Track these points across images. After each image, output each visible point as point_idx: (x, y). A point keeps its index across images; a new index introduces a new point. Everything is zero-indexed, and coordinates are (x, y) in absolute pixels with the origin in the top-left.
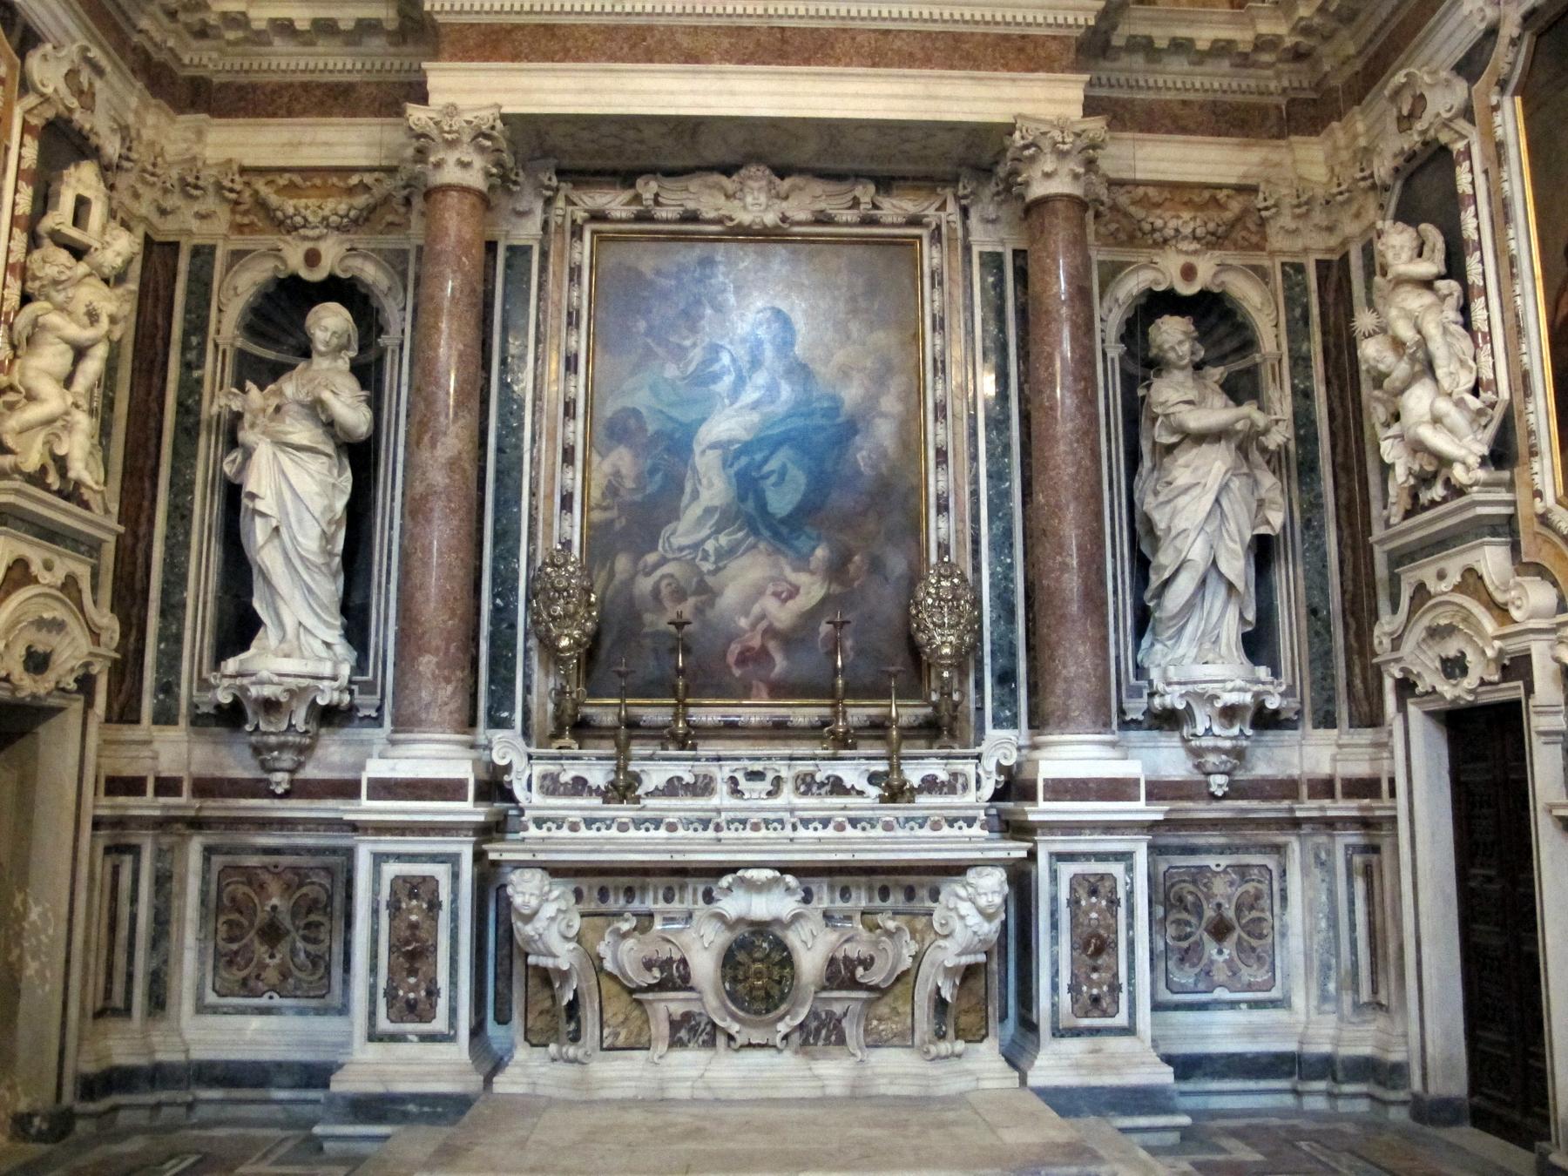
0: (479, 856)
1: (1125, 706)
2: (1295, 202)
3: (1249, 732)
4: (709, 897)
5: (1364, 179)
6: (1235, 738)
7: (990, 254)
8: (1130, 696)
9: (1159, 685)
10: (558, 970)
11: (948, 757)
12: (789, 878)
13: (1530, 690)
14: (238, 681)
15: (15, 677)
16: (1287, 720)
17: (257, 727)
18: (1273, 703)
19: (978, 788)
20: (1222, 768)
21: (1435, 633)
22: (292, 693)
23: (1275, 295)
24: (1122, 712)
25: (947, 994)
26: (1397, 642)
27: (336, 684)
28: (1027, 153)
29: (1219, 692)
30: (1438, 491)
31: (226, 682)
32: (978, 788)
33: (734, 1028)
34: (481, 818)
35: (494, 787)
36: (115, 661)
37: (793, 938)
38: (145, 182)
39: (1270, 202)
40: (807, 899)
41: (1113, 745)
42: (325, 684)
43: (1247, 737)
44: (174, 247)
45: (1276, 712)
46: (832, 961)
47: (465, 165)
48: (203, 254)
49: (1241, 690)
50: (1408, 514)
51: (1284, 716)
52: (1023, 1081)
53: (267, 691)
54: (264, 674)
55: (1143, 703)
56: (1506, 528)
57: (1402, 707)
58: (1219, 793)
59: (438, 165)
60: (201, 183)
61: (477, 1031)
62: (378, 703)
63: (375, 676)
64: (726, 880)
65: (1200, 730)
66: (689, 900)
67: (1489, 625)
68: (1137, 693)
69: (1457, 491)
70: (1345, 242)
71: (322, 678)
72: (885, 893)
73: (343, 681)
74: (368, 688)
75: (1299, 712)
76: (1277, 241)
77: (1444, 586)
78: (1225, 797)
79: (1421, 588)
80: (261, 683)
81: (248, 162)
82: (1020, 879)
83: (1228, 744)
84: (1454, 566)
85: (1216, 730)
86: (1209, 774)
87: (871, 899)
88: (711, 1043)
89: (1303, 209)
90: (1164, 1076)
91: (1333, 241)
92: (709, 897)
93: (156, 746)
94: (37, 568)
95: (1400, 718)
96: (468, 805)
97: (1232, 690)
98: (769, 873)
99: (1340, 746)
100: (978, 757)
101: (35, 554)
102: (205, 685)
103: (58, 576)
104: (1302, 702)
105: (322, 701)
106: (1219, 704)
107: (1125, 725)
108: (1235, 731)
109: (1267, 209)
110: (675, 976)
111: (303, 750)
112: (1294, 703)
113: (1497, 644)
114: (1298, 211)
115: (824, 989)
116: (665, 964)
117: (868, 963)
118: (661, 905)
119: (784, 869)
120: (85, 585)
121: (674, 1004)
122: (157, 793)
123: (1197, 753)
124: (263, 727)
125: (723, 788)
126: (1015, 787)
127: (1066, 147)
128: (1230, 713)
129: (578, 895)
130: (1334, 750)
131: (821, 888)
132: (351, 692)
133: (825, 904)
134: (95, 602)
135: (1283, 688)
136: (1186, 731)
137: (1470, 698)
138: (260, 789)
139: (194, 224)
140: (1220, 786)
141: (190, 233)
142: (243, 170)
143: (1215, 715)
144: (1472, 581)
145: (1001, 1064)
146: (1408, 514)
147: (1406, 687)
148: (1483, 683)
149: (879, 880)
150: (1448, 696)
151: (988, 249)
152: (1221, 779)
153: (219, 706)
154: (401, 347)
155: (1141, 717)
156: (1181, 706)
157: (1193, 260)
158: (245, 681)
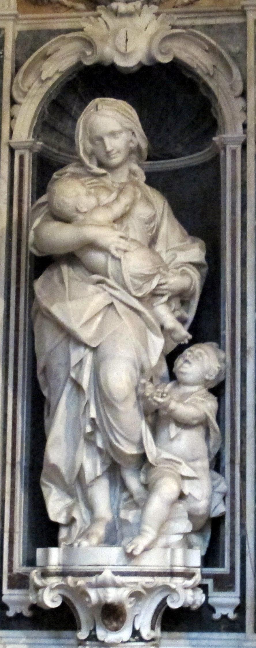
17: (93, 637)
22: (136, 595)
27: (190, 583)
31: (54, 581)
42: (177, 582)
54: (107, 574)
62: (237, 601)
63: (232, 568)
80: (103, 585)
105: (174, 604)
124: (101, 634)
132: (204, 588)
158: (81, 582)
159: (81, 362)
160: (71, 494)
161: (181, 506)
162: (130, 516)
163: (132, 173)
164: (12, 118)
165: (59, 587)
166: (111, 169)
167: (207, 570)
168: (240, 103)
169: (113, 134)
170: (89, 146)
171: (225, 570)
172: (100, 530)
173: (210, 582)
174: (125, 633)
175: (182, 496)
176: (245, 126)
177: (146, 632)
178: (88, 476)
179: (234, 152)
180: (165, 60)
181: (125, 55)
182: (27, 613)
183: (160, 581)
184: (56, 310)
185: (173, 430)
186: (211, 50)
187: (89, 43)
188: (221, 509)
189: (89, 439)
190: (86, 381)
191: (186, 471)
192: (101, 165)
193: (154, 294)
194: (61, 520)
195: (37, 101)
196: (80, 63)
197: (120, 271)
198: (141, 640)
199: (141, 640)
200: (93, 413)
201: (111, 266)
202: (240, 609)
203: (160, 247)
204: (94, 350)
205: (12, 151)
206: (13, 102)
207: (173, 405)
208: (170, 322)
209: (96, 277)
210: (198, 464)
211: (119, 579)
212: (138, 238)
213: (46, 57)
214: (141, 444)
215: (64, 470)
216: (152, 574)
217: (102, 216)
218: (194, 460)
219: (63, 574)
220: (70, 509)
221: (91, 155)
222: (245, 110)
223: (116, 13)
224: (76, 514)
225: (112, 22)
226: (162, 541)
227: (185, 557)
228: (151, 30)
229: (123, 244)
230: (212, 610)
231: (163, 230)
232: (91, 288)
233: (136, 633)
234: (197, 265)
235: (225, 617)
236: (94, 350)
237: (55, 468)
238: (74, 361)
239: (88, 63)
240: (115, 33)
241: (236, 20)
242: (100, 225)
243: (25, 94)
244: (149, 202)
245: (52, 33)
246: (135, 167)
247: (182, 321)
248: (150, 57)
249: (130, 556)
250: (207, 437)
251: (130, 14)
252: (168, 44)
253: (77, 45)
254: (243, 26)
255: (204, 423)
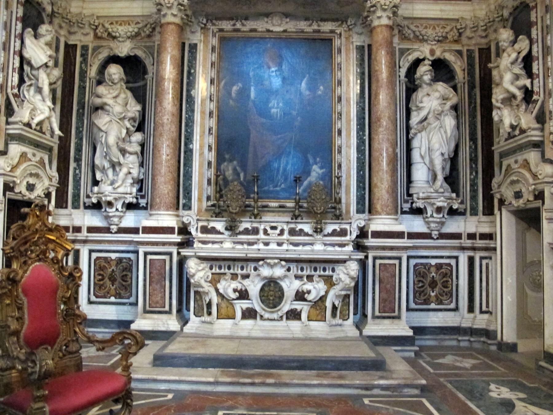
0: (179, 253)
1: (403, 206)
2: (472, 26)
3: (446, 216)
4: (256, 269)
5: (498, 17)
6: (440, 218)
7: (360, 46)
8: (404, 203)
9: (415, 199)
10: (204, 292)
11: (340, 223)
12: (283, 263)
13: (543, 203)
14: (99, 195)
15: (23, 192)
16: (461, 212)
17: (106, 211)
18: (455, 207)
19: (350, 235)
20: (436, 229)
21: (513, 183)
22: (116, 199)
23: (464, 61)
24: (402, 208)
25: (336, 303)
26: (499, 186)
27: (131, 196)
28: (372, 9)
29: (435, 202)
30: (517, 132)
31: (95, 195)
32: (350, 235)
33: (263, 313)
34: (179, 240)
35: (184, 230)
36: (57, 188)
37: (284, 284)
38: (64, 22)
39: (463, 26)
40: (289, 270)
41: (396, 219)
42: (128, 196)
43: (446, 219)
44: (76, 46)
45: (457, 209)
46: (298, 292)
47: (175, 16)
48: (85, 48)
49: (443, 201)
50: (506, 140)
51: (459, 211)
52: (361, 333)
53: (109, 199)
55: (408, 205)
56: (538, 145)
57: (500, 209)
58: (435, 237)
59: (164, 16)
60: (83, 22)
61: (179, 311)
64: (261, 263)
65: (429, 215)
66: (249, 269)
67: (531, 181)
68: (406, 202)
69: (523, 131)
70: (490, 41)
71: (127, 194)
72: (315, 270)
73: (134, 194)
74: (143, 197)
75: (465, 210)
76: (464, 40)
77: (516, 166)
78: (437, 239)
79: (509, 166)
80: (106, 196)
81: (99, 15)
82: (363, 264)
83: (438, 220)
84: (520, 158)
85: (435, 215)
86: (432, 230)
87: (311, 271)
88: (255, 318)
89: (475, 29)
90: (410, 333)
91: (484, 41)
92: (256, 269)
93: (73, 216)
94: (30, 156)
95: (499, 212)
96: (175, 236)
97: (440, 201)
98: (276, 261)
99: (479, 222)
100: (351, 223)
101: (29, 150)
102: (88, 197)
103: (38, 159)
104: (466, 206)
106: (435, 207)
107: (403, 213)
108: (441, 216)
109: (461, 28)
110: (243, 295)
111: (121, 217)
112: (463, 206)
113: (533, 187)
114: (473, 29)
115: (294, 300)
116: (240, 292)
117: (309, 292)
118: (239, 271)
119: (281, 259)
120: (47, 161)
121: (244, 304)
122: (73, 232)
123: (428, 223)
124: (107, 209)
125: (261, 232)
126: (363, 233)
127: (386, 7)
128: (439, 210)
129: (211, 268)
130: (477, 223)
131: (293, 266)
132: (137, 198)
133: (295, 272)
134: (51, 168)
135: (459, 201)
136: (425, 215)
137: (523, 206)
138: (107, 230)
139: (83, 38)
140: (436, 235)
141: (80, 41)
142: (98, 17)
143: (434, 211)
144: (526, 164)
145: (354, 328)
146: (506, 140)
147: (502, 202)
148: (528, 201)
149: (314, 265)
150: (516, 205)
151: (359, 44)
152: (437, 233)
153: (93, 203)
154: (153, 79)
155: (408, 210)
156: (422, 207)
157: (434, 47)
158: (101, 195)
159: (102, 136)
160: (103, 173)
161: (129, 176)
162: (115, 178)
163: (121, 85)
164: (90, 70)
165: (96, 197)
166: (115, 84)
167: (138, 193)
168: (152, 67)
169: (114, 74)
170: (108, 77)
171: (143, 193)
172: (109, 182)
173: (139, 197)
174: (114, 209)
175: (130, 173)
176: (153, 73)
177: (120, 209)
178: (106, 168)
179: (150, 81)
180: (132, 54)
181: (121, 53)
182: (91, 205)
183: (123, 195)
184: (96, 122)
185: (127, 155)
186: (145, 52)
187: (111, 49)
188: (142, 177)
189: (105, 157)
190: (103, 141)
191: (131, 166)
192: (112, 83)
193: (124, 118)
194: (100, 180)
195: (97, 66)
196: (109, 55)
197: (113, 111)
198: (119, 211)
199: (119, 211)
200: (105, 150)
201: (111, 110)
202: (147, 204)
203: (128, 106)
204: (106, 133)
205: (90, 79)
206: (91, 66)
207: (126, 148)
208: (129, 125)
209: (107, 113)
210: (135, 165)
211: (110, 194)
212: (121, 103)
213: (100, 53)
214: (118, 159)
215: (100, 166)
216: (121, 193)
217: (110, 96)
218: (134, 163)
219: (97, 194)
220: (102, 177)
221: (110, 80)
222: (153, 69)
223: (120, 41)
224: (103, 178)
225: (118, 44)
226: (124, 185)
227: (131, 189)
228: (129, 46)
229: (114, 104)
230: (140, 204)
231: (129, 102)
232: (106, 116)
233: (117, 210)
234: (139, 111)
235: (143, 206)
236: (106, 133)
237: (97, 165)
238: (101, 135)
239: (111, 55)
240: (119, 47)
241: (152, 44)
242: (108, 98)
243: (94, 63)
244: (125, 93)
245: (102, 46)
246: (123, 84)
247: (133, 126)
248: (128, 53)
249: (114, 189)
250: (138, 157)
251: (123, 42)
252: (133, 50)
253: (108, 50)
254: (154, 46)
255: (136, 153)
